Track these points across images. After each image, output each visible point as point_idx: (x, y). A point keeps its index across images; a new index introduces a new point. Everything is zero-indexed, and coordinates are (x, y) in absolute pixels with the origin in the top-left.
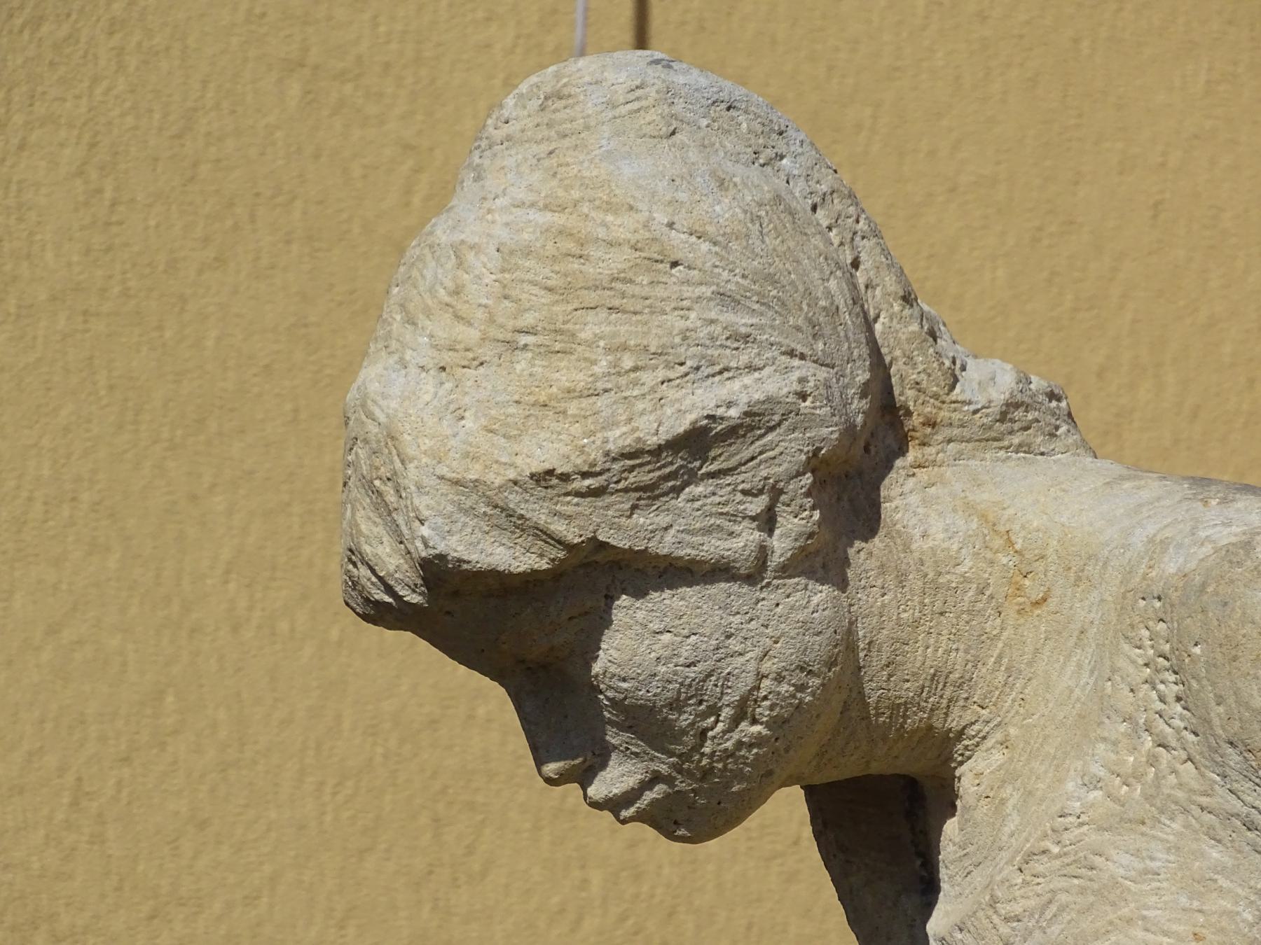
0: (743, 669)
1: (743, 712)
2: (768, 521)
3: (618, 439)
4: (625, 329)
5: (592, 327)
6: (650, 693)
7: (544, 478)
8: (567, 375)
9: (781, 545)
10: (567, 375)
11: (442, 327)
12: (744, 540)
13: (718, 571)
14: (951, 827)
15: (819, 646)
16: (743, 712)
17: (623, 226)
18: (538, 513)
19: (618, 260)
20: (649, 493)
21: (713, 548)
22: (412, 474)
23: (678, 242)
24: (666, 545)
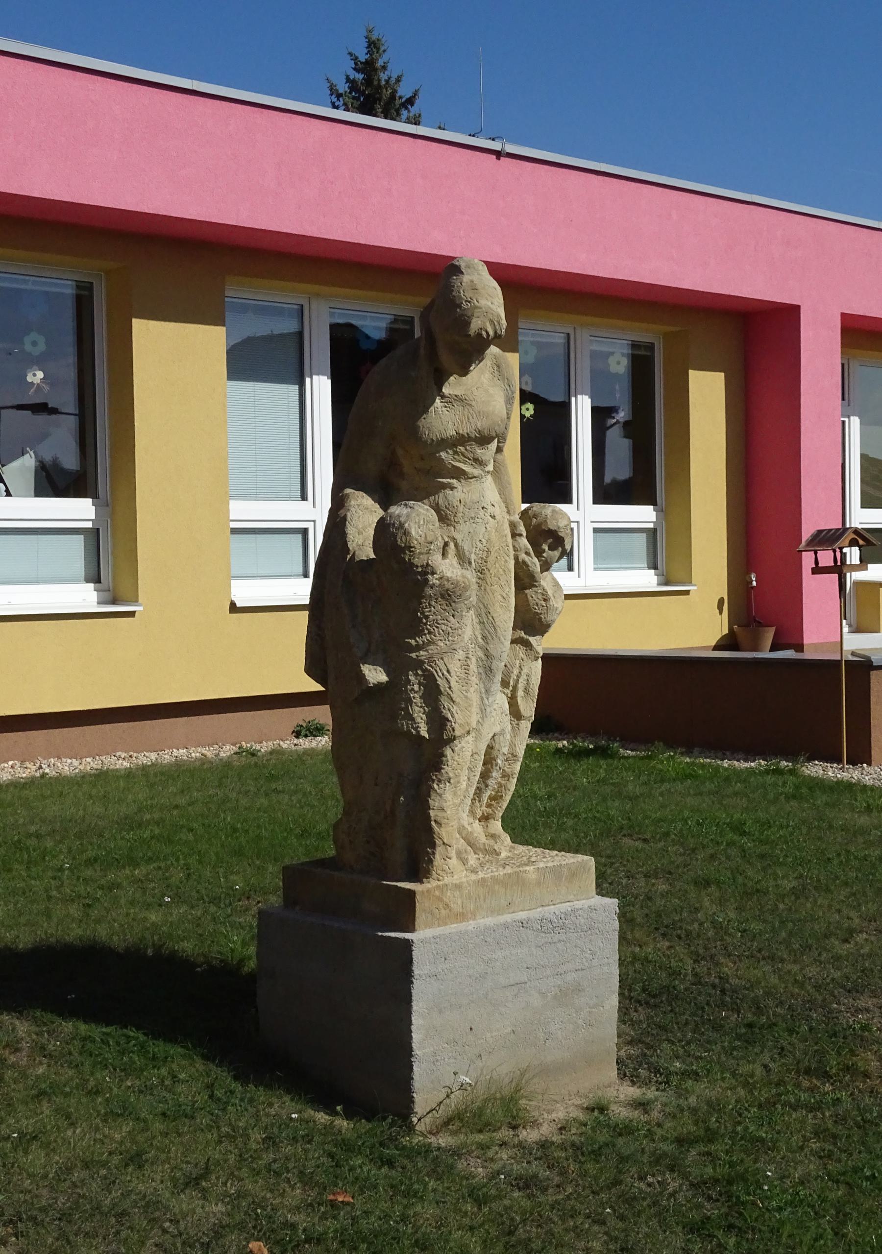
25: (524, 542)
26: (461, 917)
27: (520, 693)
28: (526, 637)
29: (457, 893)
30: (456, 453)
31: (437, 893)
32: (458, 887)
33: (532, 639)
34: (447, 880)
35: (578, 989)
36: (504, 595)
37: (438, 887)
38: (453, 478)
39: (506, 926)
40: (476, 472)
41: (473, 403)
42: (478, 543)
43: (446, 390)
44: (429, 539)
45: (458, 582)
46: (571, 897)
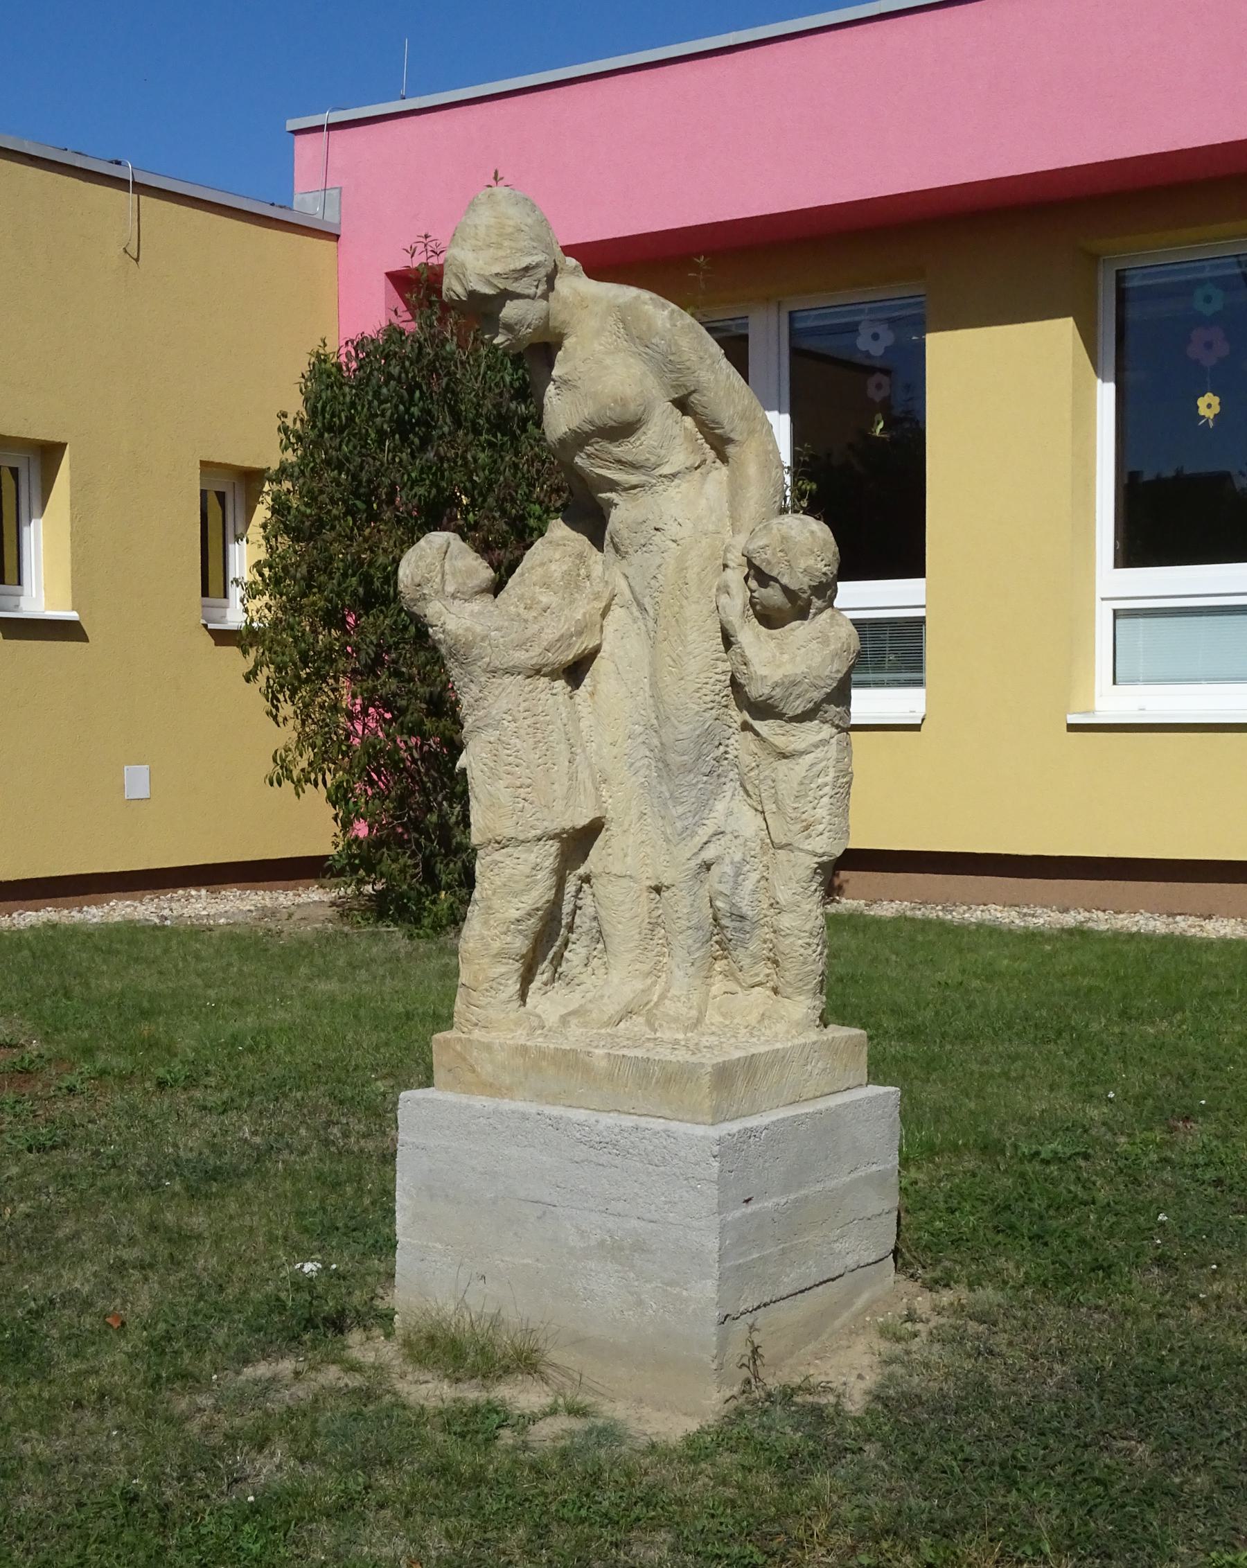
0: (530, 317)
1: (528, 327)
2: (537, 287)
3: (512, 267)
4: (513, 244)
5: (506, 243)
6: (512, 321)
7: (497, 274)
8: (501, 253)
9: (539, 292)
10: (501, 253)
11: (474, 242)
12: (532, 291)
13: (528, 297)
14: (560, 353)
15: (543, 314)
16: (528, 327)
17: (511, 223)
18: (495, 281)
19: (510, 230)
20: (516, 279)
21: (526, 292)
22: (468, 273)
23: (523, 227)
24: (518, 290)
25: (735, 577)
26: (491, 1088)
27: (770, 807)
28: (751, 721)
29: (485, 1055)
30: (589, 456)
31: (458, 1048)
32: (488, 1047)
33: (757, 725)
34: (477, 1034)
35: (640, 1247)
36: (674, 656)
37: (460, 1039)
38: (611, 491)
39: (525, 1117)
40: (633, 479)
41: (579, 383)
42: (653, 582)
43: (555, 373)
44: (417, 580)
45: (457, 636)
46: (667, 1113)
